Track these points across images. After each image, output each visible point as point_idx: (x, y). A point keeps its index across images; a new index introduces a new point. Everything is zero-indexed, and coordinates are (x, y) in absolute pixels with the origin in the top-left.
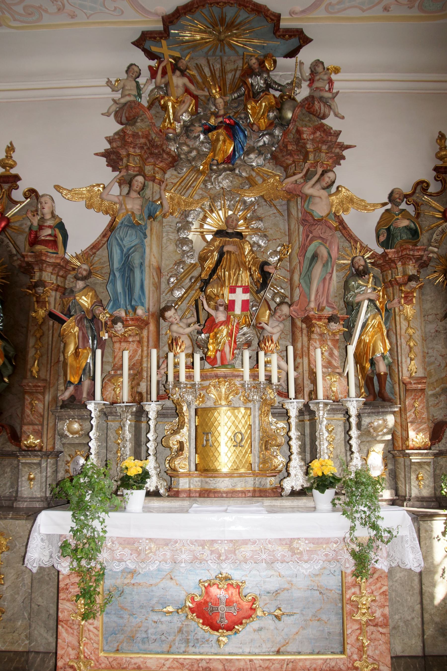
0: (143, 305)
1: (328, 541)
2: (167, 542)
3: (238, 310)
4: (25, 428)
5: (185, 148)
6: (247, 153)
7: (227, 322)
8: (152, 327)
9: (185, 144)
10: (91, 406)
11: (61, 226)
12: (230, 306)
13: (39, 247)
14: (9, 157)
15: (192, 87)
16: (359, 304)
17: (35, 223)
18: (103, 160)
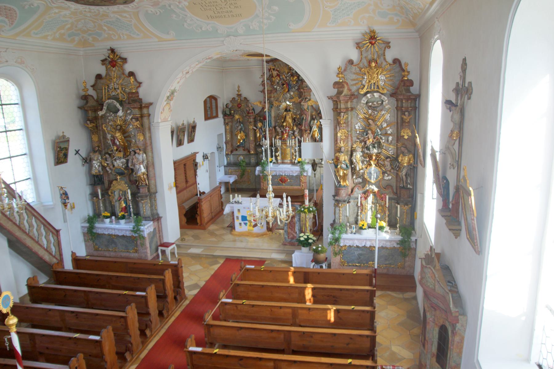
0: (271, 126)
1: (297, 171)
2: (275, 171)
3: (287, 131)
4: (251, 150)
5: (278, 87)
6: (292, 88)
7: (286, 133)
8: (273, 129)
9: (278, 86)
10: (263, 148)
11: (253, 109)
12: (286, 130)
13: (249, 115)
14: (239, 89)
15: (278, 73)
16: (312, 127)
17: (248, 110)
18: (260, 92)
